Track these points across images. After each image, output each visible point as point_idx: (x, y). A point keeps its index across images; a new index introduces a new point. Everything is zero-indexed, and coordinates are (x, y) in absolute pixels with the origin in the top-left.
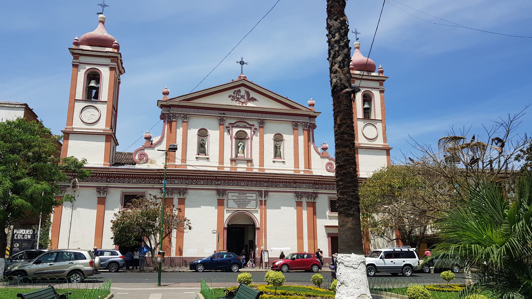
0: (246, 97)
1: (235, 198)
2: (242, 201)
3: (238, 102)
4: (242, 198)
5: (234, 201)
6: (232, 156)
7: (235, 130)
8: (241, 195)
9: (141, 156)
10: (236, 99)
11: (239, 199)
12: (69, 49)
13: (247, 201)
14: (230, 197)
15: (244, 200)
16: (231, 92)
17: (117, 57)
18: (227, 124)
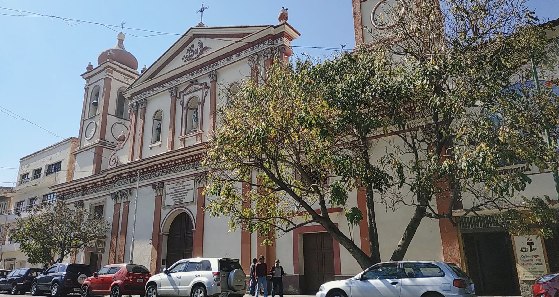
0: (199, 51)
1: (172, 191)
2: (179, 194)
3: (191, 61)
4: (180, 189)
5: (171, 196)
6: (181, 135)
7: (187, 98)
8: (179, 186)
9: (114, 160)
10: (189, 58)
11: (176, 191)
12: (82, 75)
13: (184, 192)
14: (168, 191)
15: (181, 191)
16: (184, 53)
17: (108, 67)
18: (178, 96)
